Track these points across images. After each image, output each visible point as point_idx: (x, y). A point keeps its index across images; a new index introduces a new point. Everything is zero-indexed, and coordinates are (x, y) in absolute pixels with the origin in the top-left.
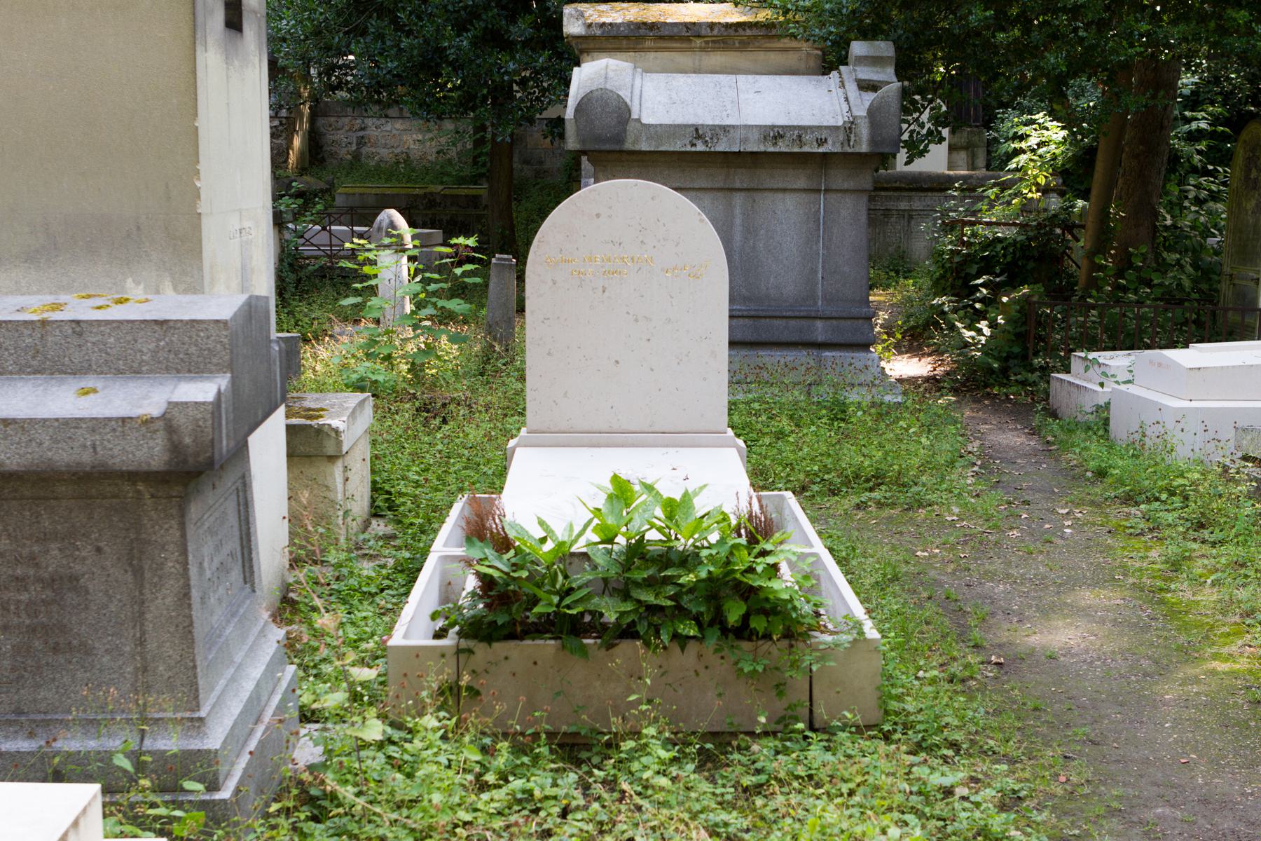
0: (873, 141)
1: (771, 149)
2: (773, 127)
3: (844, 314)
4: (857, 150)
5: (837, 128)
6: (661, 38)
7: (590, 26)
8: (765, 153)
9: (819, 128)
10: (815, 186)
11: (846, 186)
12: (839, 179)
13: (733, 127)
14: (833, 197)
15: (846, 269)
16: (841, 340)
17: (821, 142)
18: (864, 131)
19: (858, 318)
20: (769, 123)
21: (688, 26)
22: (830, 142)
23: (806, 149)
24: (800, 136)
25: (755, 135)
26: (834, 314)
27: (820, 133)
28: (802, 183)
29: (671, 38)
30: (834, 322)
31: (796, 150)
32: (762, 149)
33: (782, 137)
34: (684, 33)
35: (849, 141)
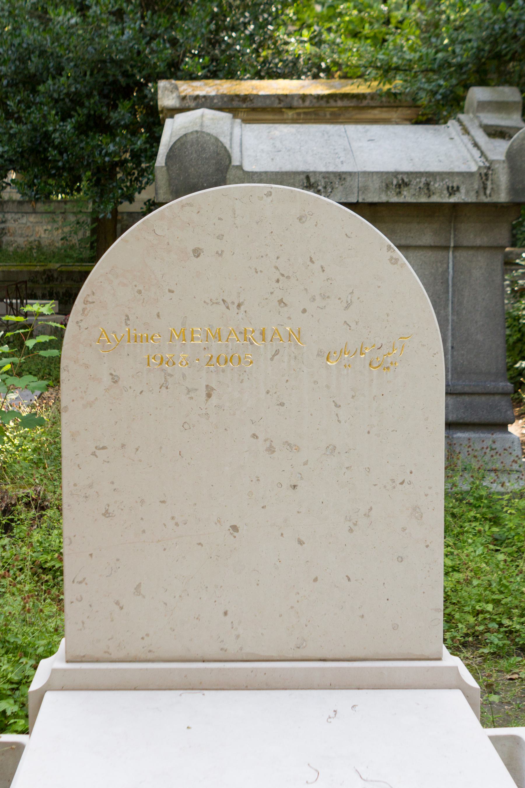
0: (513, 189)
1: (395, 199)
2: (396, 174)
3: (478, 389)
4: (494, 199)
5: (471, 174)
6: (254, 110)
7: (184, 98)
8: (387, 205)
9: (451, 174)
10: (443, 243)
11: (478, 242)
12: (471, 234)
13: (350, 174)
14: (463, 255)
15: (480, 337)
16: (475, 419)
17: (453, 191)
18: (502, 178)
19: (494, 394)
20: (391, 168)
21: (280, 98)
22: (463, 190)
23: (435, 199)
24: (428, 184)
25: (375, 184)
26: (467, 389)
27: (452, 180)
28: (427, 238)
29: (264, 110)
30: (467, 398)
31: (423, 199)
32: (384, 199)
33: (406, 185)
34: (276, 105)
35: (485, 188)
